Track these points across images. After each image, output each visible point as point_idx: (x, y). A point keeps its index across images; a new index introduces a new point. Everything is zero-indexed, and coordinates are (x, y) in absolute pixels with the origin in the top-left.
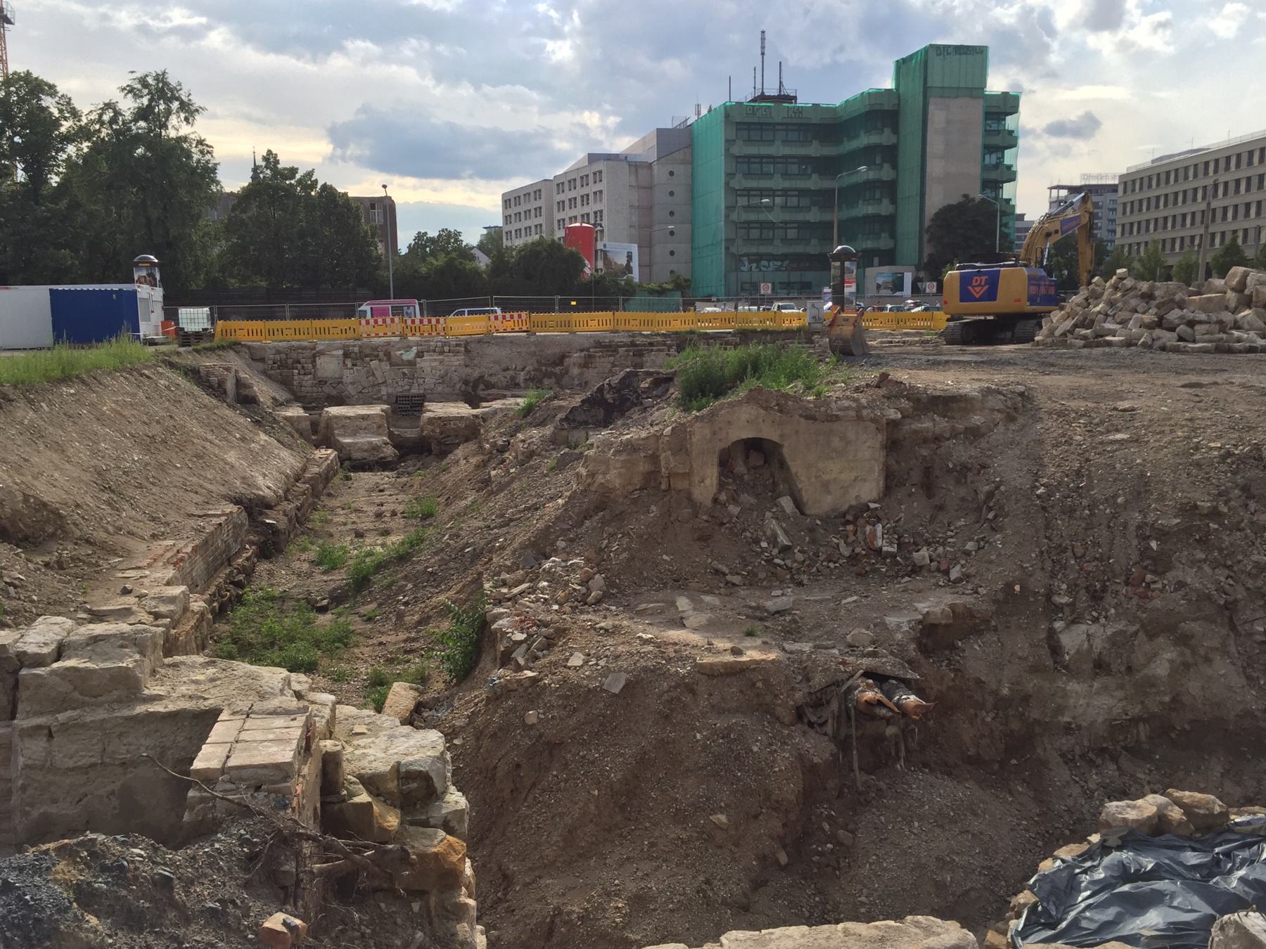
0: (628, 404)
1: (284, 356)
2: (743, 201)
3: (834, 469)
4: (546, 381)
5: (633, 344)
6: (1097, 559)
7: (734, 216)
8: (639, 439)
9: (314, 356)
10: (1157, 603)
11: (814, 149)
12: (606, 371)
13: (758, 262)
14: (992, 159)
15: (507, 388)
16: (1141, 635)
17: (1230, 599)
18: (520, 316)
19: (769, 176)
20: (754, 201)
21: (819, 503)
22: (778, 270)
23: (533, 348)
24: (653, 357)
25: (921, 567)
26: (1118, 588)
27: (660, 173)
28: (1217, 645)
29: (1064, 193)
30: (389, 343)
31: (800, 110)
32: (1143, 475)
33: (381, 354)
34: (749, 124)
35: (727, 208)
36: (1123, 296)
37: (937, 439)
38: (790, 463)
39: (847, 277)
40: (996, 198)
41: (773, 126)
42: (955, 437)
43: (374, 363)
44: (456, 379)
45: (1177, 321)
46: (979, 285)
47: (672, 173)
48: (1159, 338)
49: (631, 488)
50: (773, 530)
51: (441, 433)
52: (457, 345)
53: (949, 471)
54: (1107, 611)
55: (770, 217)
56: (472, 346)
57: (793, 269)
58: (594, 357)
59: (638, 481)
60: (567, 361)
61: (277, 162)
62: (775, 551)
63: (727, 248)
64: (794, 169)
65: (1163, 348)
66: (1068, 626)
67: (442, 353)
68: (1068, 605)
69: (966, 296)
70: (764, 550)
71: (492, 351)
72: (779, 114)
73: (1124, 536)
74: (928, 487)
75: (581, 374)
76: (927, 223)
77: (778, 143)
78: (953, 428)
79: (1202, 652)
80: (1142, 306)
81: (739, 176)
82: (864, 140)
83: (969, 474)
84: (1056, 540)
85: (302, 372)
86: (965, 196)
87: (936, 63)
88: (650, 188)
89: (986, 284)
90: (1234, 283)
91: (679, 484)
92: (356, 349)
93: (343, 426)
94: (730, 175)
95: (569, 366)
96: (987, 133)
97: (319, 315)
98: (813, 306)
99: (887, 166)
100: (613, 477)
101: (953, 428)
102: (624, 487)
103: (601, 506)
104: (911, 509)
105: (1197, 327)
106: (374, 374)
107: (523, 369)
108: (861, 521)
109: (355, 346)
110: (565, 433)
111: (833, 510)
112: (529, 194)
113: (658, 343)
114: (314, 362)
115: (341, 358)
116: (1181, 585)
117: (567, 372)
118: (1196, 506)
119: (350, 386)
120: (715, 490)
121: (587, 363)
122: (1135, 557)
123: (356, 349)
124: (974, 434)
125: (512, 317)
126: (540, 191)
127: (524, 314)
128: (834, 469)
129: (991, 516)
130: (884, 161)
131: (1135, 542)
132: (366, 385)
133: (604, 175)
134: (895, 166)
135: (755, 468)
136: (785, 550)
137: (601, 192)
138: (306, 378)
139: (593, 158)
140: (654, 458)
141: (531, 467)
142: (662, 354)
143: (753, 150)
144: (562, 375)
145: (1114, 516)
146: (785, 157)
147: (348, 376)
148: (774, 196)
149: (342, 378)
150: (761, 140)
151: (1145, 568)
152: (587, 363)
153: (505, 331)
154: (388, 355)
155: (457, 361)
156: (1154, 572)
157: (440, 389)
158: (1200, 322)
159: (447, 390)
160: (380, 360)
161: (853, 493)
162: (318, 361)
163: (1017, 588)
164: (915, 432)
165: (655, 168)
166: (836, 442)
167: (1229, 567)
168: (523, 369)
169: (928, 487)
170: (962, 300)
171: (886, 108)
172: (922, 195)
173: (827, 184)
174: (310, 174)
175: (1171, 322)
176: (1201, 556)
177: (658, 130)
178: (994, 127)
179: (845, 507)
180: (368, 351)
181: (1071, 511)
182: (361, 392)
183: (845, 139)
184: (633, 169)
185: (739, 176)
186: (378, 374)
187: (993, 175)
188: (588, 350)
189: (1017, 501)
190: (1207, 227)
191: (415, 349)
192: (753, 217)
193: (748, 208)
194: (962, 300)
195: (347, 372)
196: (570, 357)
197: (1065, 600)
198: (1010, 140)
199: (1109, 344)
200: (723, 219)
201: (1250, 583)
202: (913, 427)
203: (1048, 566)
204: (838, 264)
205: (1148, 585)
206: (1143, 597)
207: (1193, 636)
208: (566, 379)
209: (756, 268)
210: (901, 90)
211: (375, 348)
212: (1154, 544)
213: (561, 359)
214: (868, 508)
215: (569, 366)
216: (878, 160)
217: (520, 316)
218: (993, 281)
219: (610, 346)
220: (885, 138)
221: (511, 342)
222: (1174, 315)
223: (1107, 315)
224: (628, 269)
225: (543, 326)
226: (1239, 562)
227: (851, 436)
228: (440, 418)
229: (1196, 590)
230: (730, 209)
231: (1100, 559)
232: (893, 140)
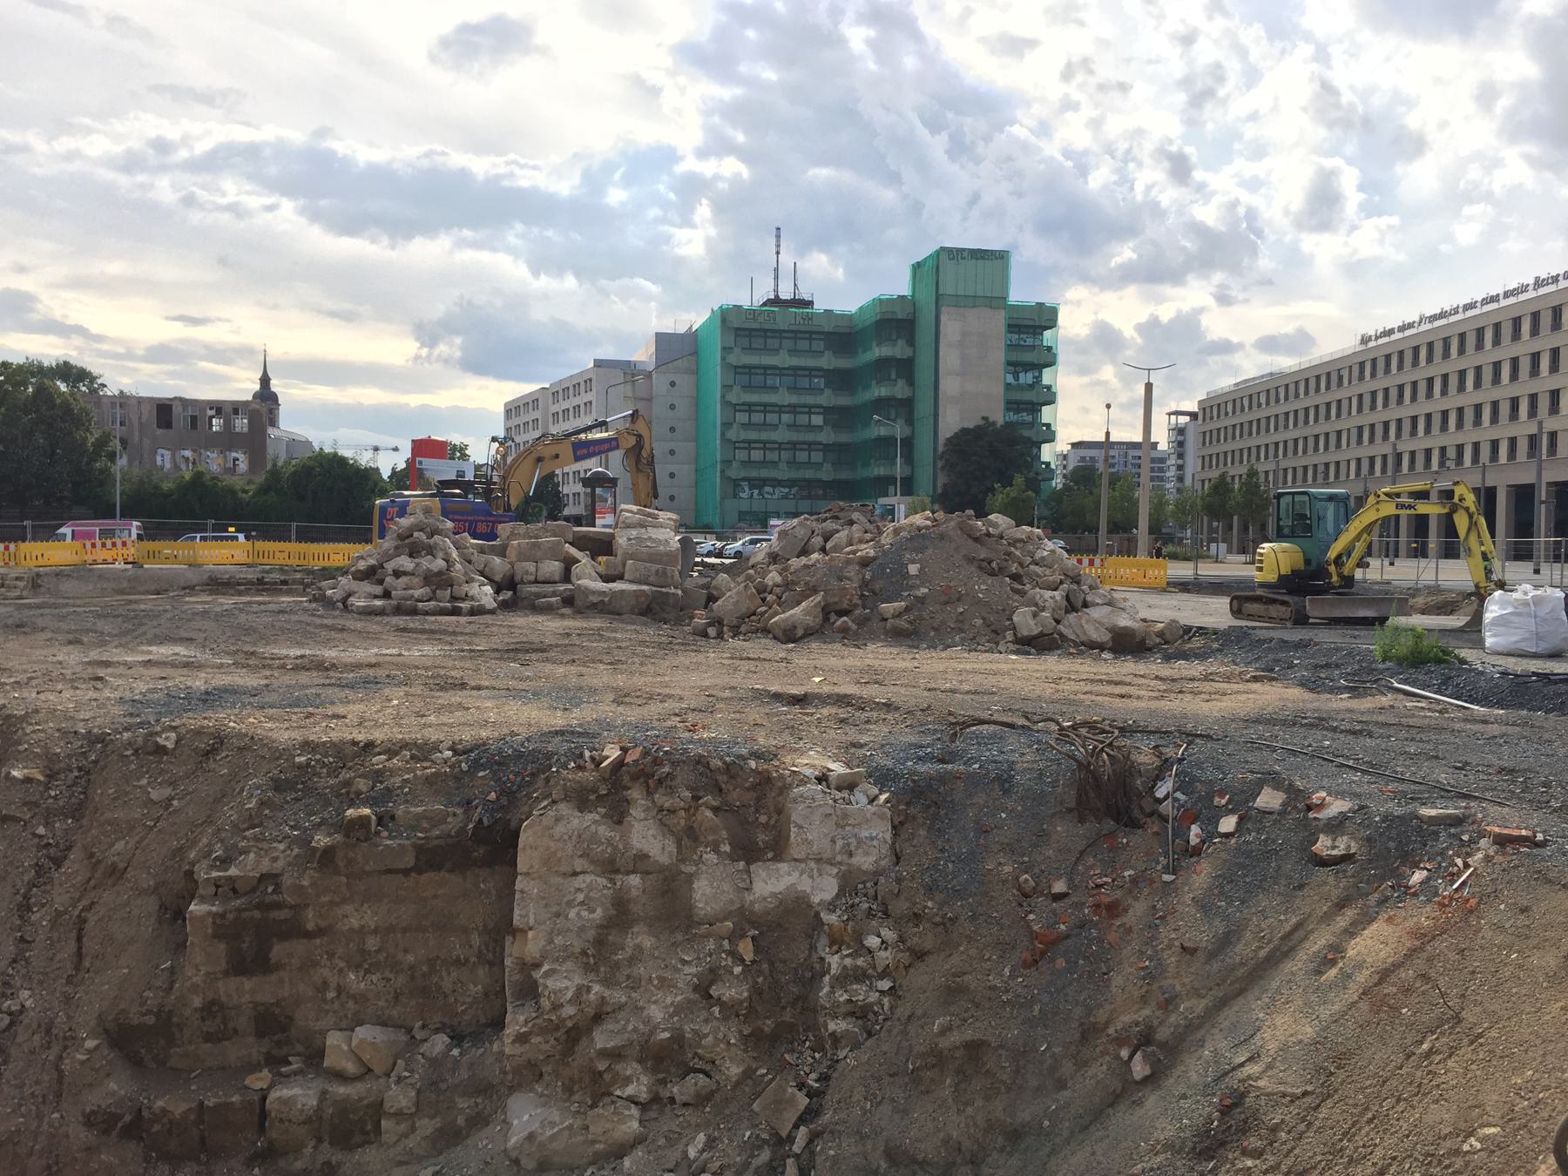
2: (742, 417)
7: (732, 434)
11: (828, 361)
13: (760, 488)
20: (757, 418)
22: (785, 497)
27: (660, 384)
29: (1183, 420)
39: (598, 506)
40: (1032, 425)
47: (673, 384)
55: (776, 436)
76: (941, 449)
81: (736, 389)
82: (878, 351)
94: (726, 388)
99: (901, 383)
130: (898, 377)
139: (599, 364)
146: (795, 369)
148: (780, 412)
150: (765, 349)
158: (405, 573)
172: (936, 415)
173: (843, 401)
185: (736, 389)
192: (753, 435)
193: (748, 426)
198: (1049, 359)
210: (917, 296)
216: (893, 376)
220: (899, 350)
230: (726, 425)
232: (908, 352)
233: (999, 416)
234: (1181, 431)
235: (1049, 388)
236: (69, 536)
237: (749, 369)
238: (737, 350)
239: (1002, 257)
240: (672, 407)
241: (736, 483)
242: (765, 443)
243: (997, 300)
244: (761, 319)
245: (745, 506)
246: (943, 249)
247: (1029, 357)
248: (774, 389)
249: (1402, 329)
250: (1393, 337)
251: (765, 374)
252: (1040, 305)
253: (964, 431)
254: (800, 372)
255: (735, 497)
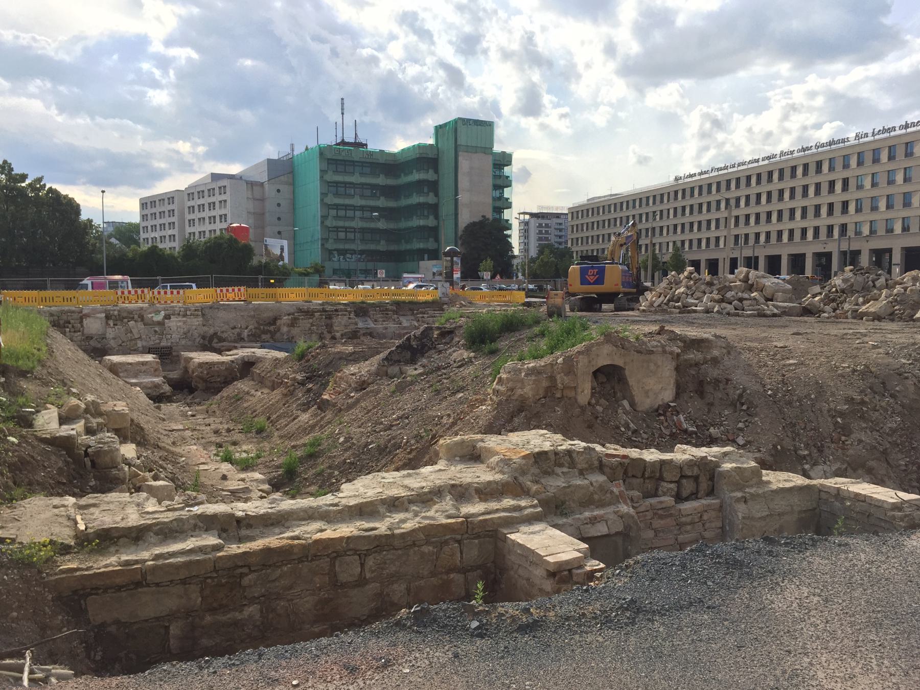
0: (426, 348)
1: (56, 318)
3: (651, 383)
4: (264, 337)
5: (324, 310)
6: (812, 429)
8: (540, 366)
9: (81, 319)
10: (851, 452)
11: (381, 180)
12: (307, 329)
14: (497, 194)
15: (235, 341)
16: (849, 469)
17: (884, 447)
18: (239, 290)
19: (351, 196)
21: (645, 403)
23: (252, 313)
24: (340, 320)
25: (716, 439)
26: (829, 445)
28: (885, 473)
30: (142, 308)
31: (371, 154)
32: (817, 383)
33: (136, 317)
34: (337, 160)
35: (322, 217)
36: (695, 284)
37: (697, 364)
38: (628, 379)
41: (353, 163)
42: (706, 363)
43: (132, 323)
44: (196, 334)
45: (732, 298)
46: (593, 275)
48: (725, 308)
49: (538, 397)
50: (625, 421)
51: (208, 374)
52: (196, 310)
53: (709, 383)
54: (829, 458)
56: (207, 311)
57: (368, 261)
58: (299, 319)
59: (542, 393)
60: (278, 322)
61: (12, 170)
62: (630, 433)
63: (322, 245)
64: (368, 192)
65: (728, 314)
66: (812, 467)
67: (185, 315)
68: (807, 455)
69: (584, 281)
70: (624, 433)
71: (221, 314)
72: (356, 155)
73: (822, 416)
74: (701, 393)
75: (289, 332)
76: (460, 233)
77: (357, 175)
78: (705, 358)
79: (879, 477)
80: (708, 289)
82: (416, 176)
83: (721, 385)
84: (789, 420)
85: (73, 330)
86: (483, 216)
87: (462, 129)
88: (262, 200)
89: (597, 274)
90: (742, 277)
91: (571, 394)
92: (116, 313)
93: (126, 370)
94: (324, 195)
95: (280, 325)
96: (495, 177)
97: (43, 287)
98: (443, 286)
99: (431, 194)
100: (528, 390)
101: (705, 358)
102: (534, 396)
103: (520, 410)
104: (694, 406)
105: (744, 302)
106: (131, 332)
107: (247, 328)
108: (668, 414)
109: (115, 310)
110: (385, 368)
111: (650, 408)
112: (164, 200)
113: (341, 310)
114: (81, 322)
115: (104, 319)
116: (860, 441)
117: (279, 330)
118: (853, 399)
119: (112, 341)
120: (589, 397)
121: (293, 324)
122: (832, 427)
123: (116, 313)
124: (715, 361)
125: (233, 290)
126: (173, 198)
127: (242, 288)
128: (651, 383)
129: (744, 407)
131: (829, 419)
132: (125, 340)
133: (228, 189)
134: (437, 195)
135: (602, 383)
136: (635, 432)
137: (225, 201)
138: (76, 334)
140: (552, 378)
141: (372, 391)
142: (345, 318)
143: (339, 178)
144: (275, 332)
145: (813, 405)
147: (111, 333)
148: (354, 210)
149: (105, 335)
150: (345, 172)
151: (839, 433)
152: (293, 324)
153: (228, 300)
154: (142, 318)
155: (197, 322)
156: (844, 435)
157: (183, 342)
158: (746, 299)
159: (189, 343)
160: (135, 321)
161: (661, 397)
162: (85, 322)
163: (779, 447)
164: (686, 360)
165: (266, 186)
166: (652, 367)
167: (878, 431)
168: (247, 328)
169: (701, 393)
170: (581, 284)
171: (430, 156)
172: (456, 215)
173: (392, 204)
174: (39, 180)
175: (729, 299)
176: (864, 425)
177: (268, 160)
178: (497, 173)
179: (656, 406)
180: (125, 315)
181: (789, 403)
182: (121, 345)
183: (402, 175)
184: (250, 186)
186: (135, 331)
187: (498, 204)
188: (293, 314)
189: (759, 399)
190: (651, 241)
191: (163, 313)
194: (581, 284)
195: (109, 330)
196: (281, 319)
197: (806, 452)
199: (695, 311)
200: (319, 223)
201: (890, 439)
202: (685, 357)
203: (790, 434)
204: (449, 258)
205: (843, 442)
206: (843, 449)
207: (873, 469)
208: (278, 335)
209: (344, 259)
210: (439, 146)
211: (130, 312)
212: (839, 420)
213: (274, 320)
214: (670, 406)
215: (280, 325)
216: (426, 190)
217: (239, 290)
218: (602, 271)
219: (308, 312)
220: (430, 176)
221: (235, 308)
222: (729, 295)
223: (687, 295)
224: (281, 258)
225: (257, 297)
226: (882, 428)
227: (660, 363)
228: (207, 363)
229: (869, 444)
231: (815, 429)
233: (490, 215)
234: (526, 223)
235: (507, 199)
236: (90, 286)
237: (337, 184)
238: (330, 173)
239: (490, 125)
240: (279, 205)
241: (330, 252)
242: (346, 228)
243: (487, 149)
244: (343, 154)
245: (336, 266)
246: (459, 119)
247: (499, 182)
248: (352, 196)
249: (701, 174)
250: (694, 179)
251: (345, 187)
252: (504, 153)
253: (473, 224)
254: (365, 187)
255: (330, 260)
